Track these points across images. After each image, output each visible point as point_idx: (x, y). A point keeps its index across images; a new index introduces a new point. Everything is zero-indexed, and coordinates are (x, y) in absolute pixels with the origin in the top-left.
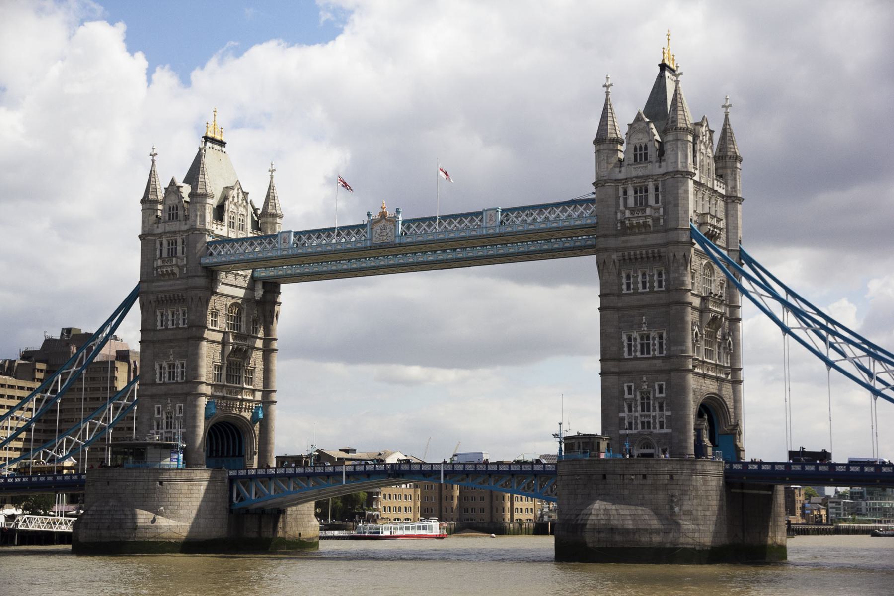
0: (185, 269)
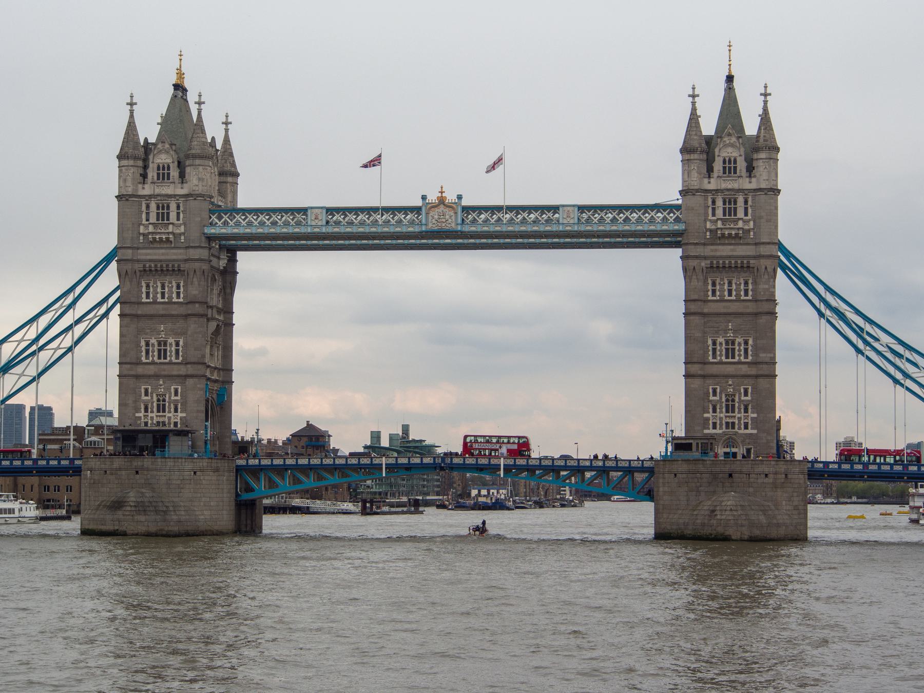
0: (182, 237)
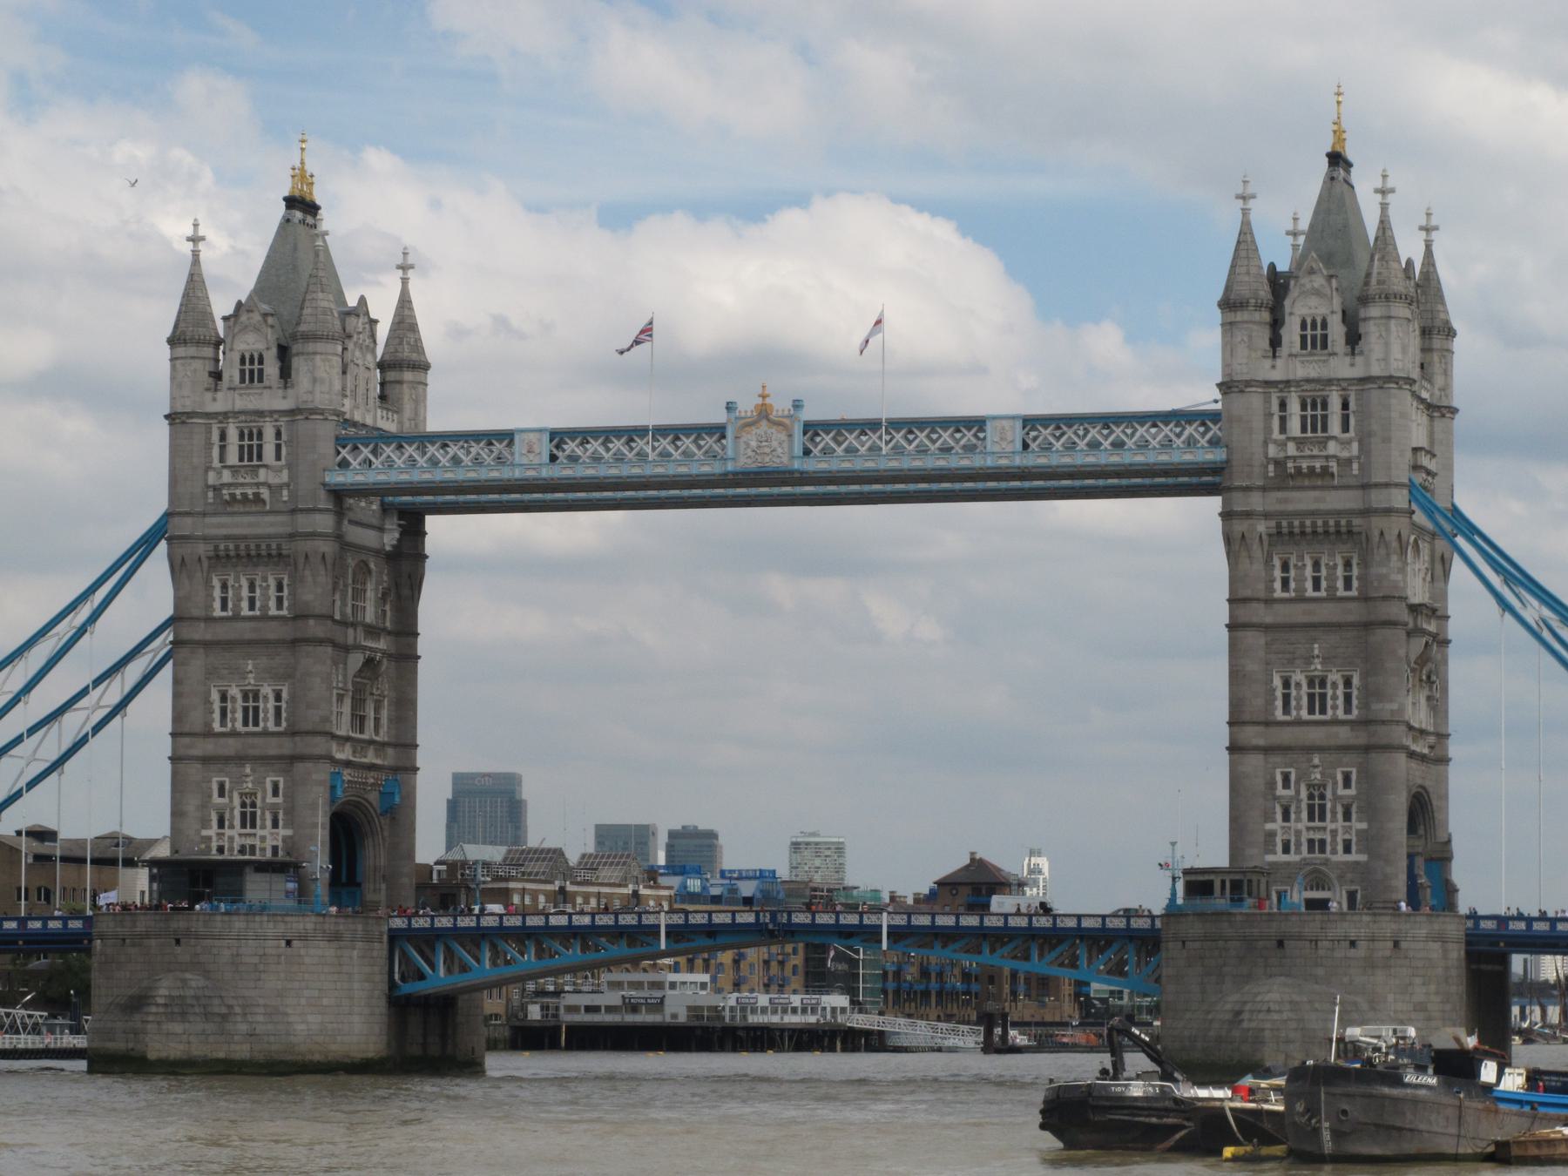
0: (285, 492)
